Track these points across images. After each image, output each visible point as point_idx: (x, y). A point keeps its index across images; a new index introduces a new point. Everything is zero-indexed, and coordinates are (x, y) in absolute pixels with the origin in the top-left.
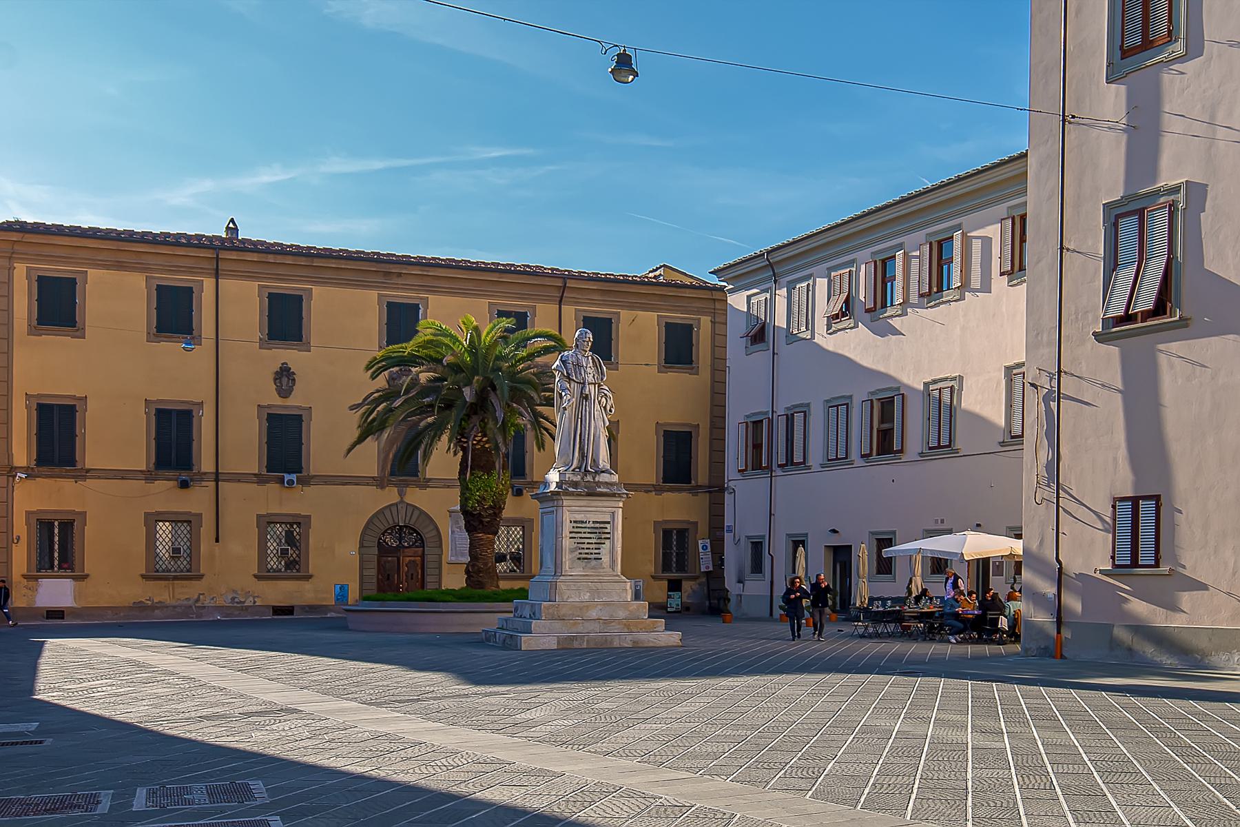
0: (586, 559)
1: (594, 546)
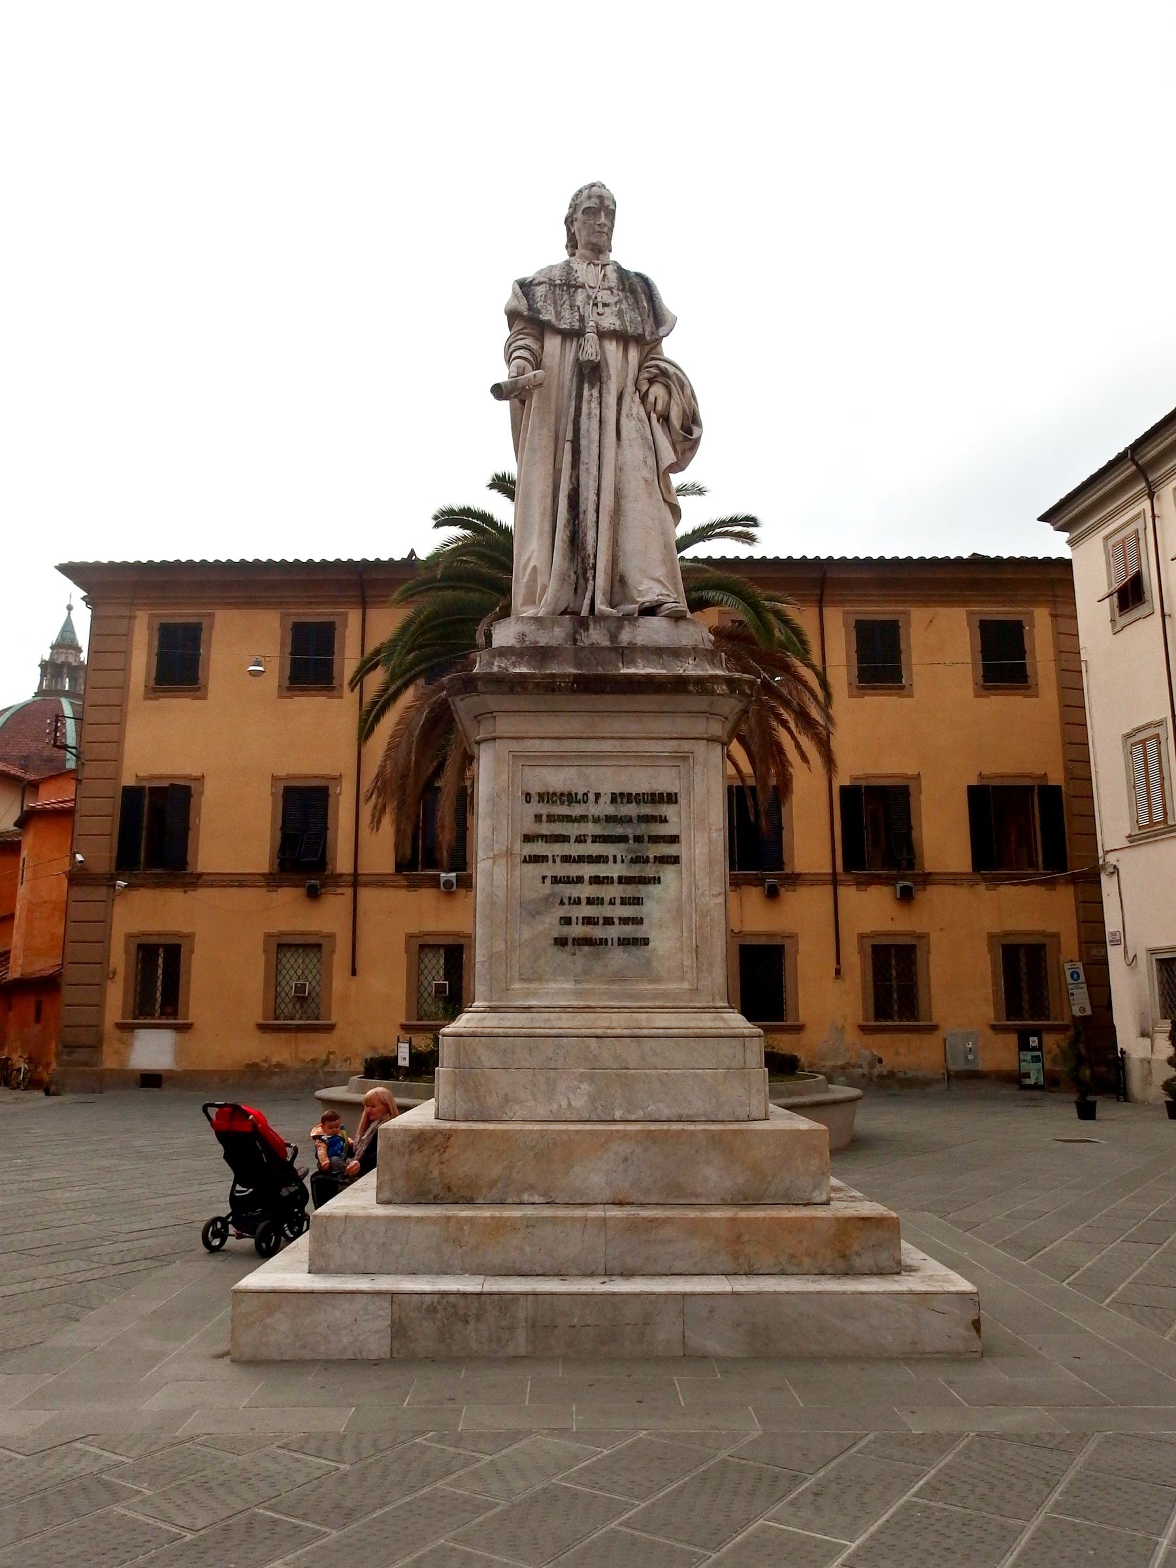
0: (588, 941)
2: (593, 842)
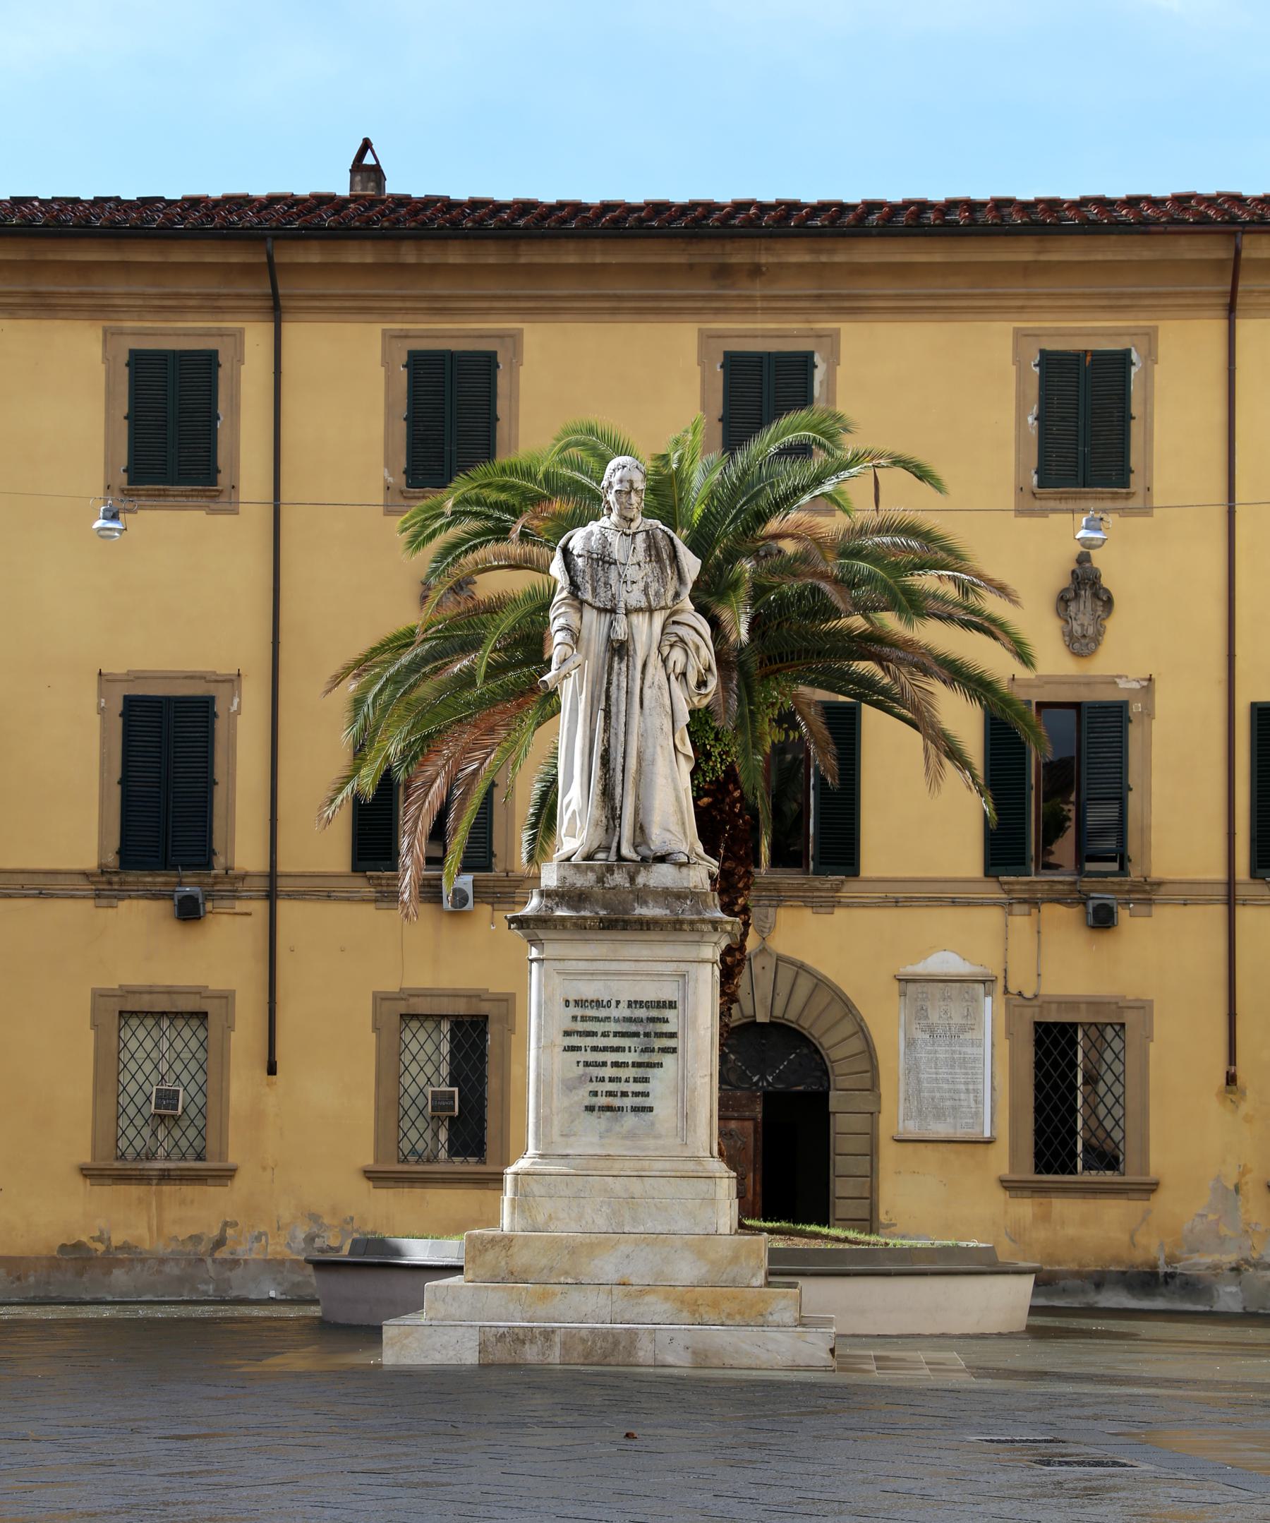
0: (609, 1108)
1: (631, 1072)
2: (615, 1036)
